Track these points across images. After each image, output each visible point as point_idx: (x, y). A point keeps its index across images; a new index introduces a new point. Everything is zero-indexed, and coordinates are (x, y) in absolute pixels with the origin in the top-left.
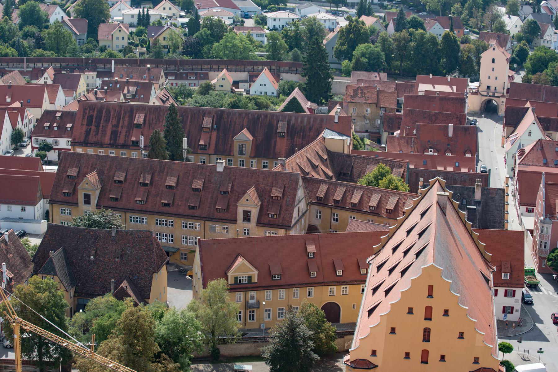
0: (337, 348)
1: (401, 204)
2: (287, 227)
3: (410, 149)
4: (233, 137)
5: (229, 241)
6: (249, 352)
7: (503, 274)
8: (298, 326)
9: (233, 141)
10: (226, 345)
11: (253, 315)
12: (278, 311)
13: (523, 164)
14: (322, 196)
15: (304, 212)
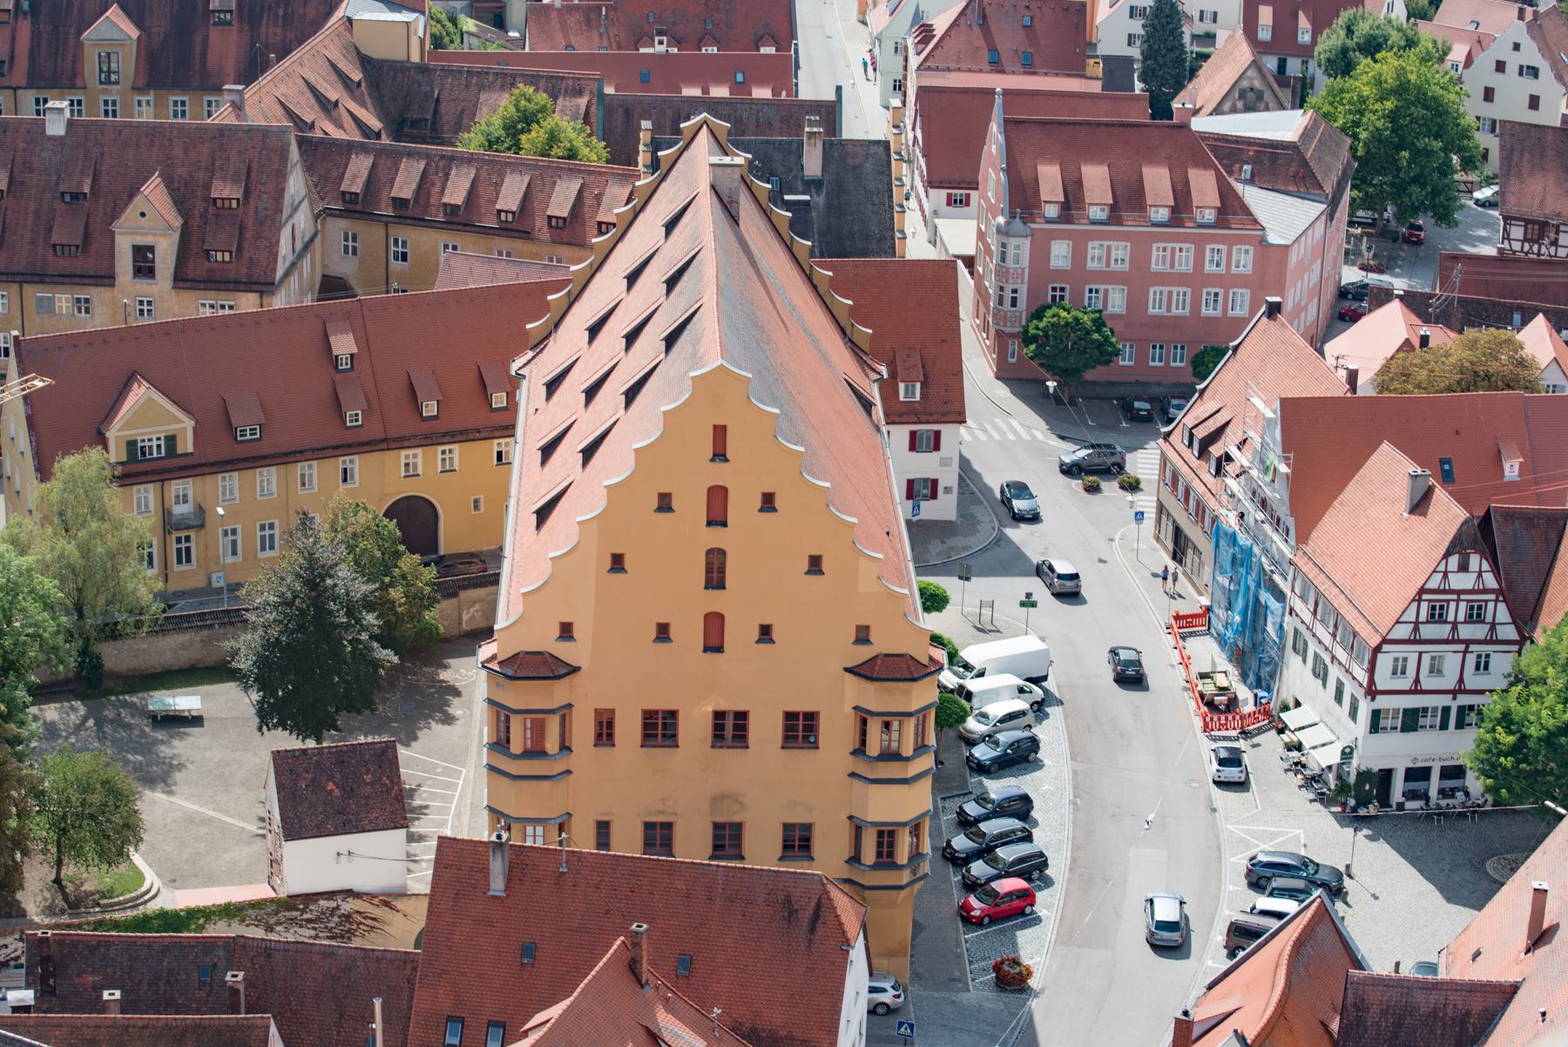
0: (442, 630)
1: (589, 200)
2: (265, 286)
3: (596, 39)
4: (80, 33)
5: (102, 338)
6: (185, 658)
7: (902, 386)
8: (328, 571)
9: (79, 45)
10: (120, 643)
11: (188, 550)
12: (259, 534)
13: (929, 68)
14: (357, 188)
15: (307, 238)
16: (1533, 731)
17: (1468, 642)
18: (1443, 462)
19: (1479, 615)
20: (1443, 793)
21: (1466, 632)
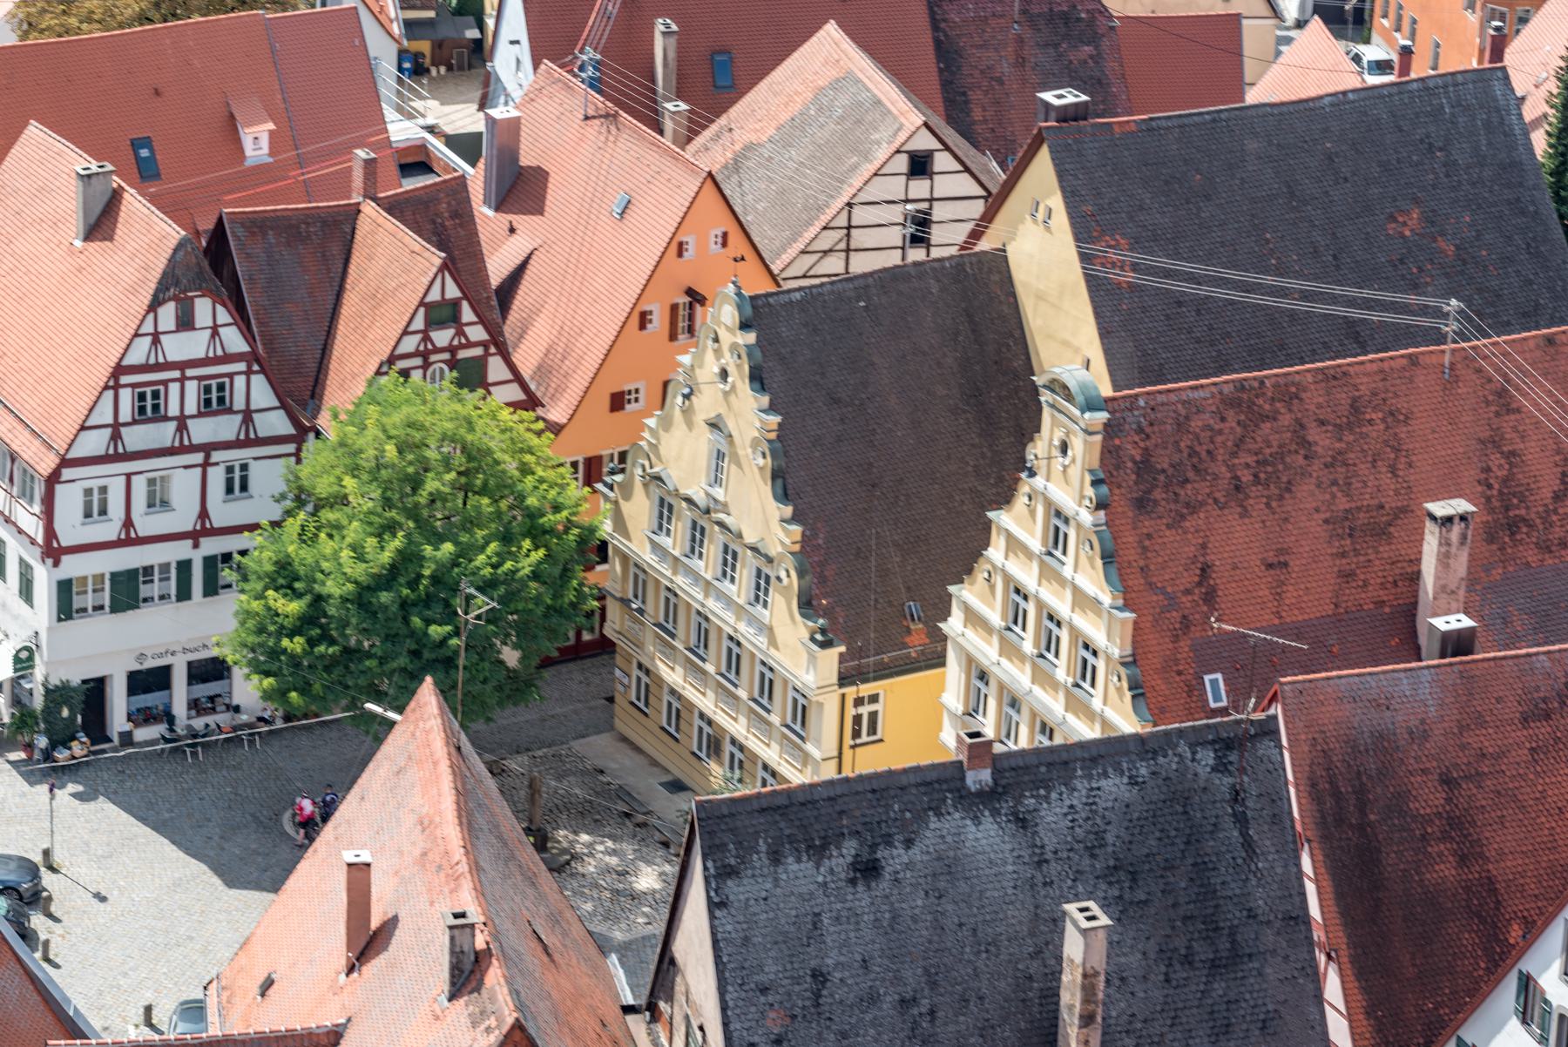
16: (332, 588)
17: (208, 448)
18: (136, 144)
19: (221, 400)
20: (195, 706)
21: (201, 430)
